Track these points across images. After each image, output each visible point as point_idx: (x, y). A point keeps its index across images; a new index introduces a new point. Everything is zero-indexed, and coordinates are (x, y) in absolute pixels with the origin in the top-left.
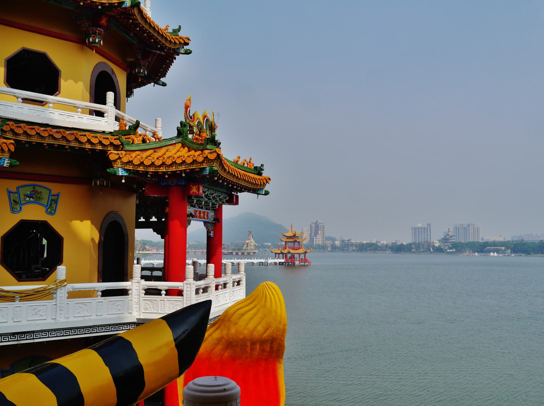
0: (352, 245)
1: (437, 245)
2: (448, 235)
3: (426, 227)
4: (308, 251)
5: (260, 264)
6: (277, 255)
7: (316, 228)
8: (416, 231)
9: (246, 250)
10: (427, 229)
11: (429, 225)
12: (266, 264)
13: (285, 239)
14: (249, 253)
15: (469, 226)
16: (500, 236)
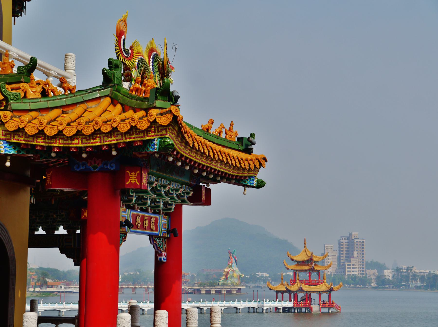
0: (415, 277)
4: (335, 287)
5: (250, 310)
6: (280, 295)
9: (224, 285)
13: (293, 266)
14: (229, 292)
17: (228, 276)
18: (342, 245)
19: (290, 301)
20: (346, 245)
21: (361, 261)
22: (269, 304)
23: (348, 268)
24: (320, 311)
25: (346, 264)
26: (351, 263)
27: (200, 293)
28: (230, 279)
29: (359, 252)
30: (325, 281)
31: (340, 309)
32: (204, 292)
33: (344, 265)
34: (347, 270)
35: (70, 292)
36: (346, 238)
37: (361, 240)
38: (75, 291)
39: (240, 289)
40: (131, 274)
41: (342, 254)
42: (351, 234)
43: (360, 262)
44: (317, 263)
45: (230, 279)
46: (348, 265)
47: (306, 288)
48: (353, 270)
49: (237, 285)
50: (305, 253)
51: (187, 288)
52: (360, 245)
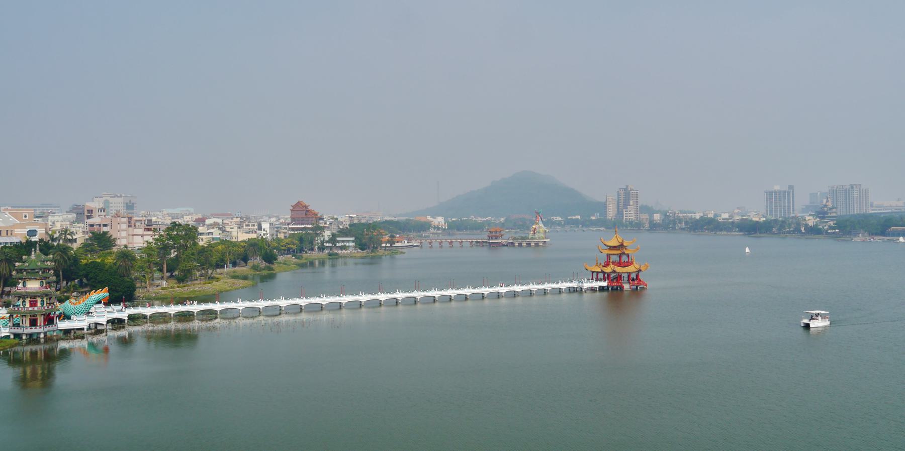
0: (680, 221)
1: (811, 224)
2: (826, 206)
3: (786, 189)
6: (595, 275)
7: (626, 197)
8: (771, 196)
9: (532, 238)
10: (788, 194)
11: (791, 187)
14: (537, 244)
15: (852, 187)
16: (899, 200)
47: (619, 269)
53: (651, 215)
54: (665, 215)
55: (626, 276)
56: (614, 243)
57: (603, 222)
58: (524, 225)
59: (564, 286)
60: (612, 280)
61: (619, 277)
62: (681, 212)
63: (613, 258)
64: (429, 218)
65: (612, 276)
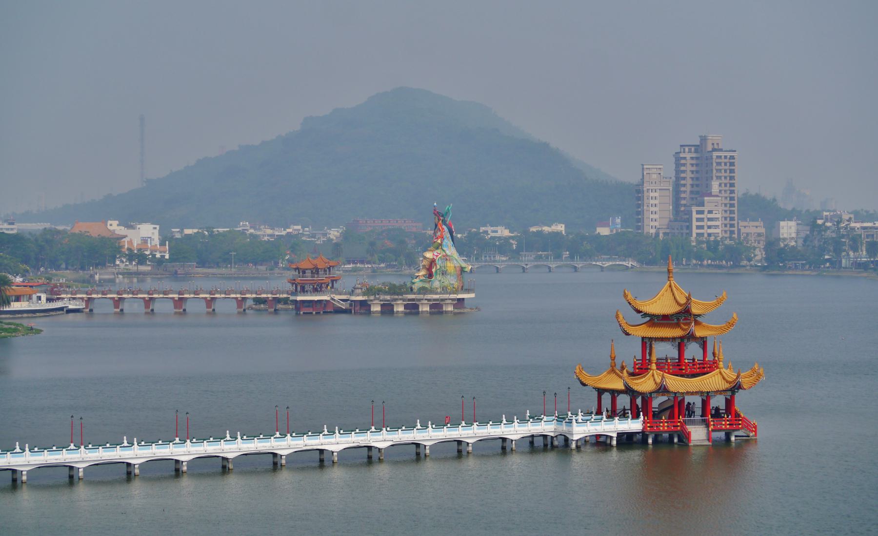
4: (745, 381)
5: (537, 446)
7: (700, 168)
9: (423, 290)
12: (560, 446)
14: (437, 307)
17: (434, 270)
18: (684, 165)
19: (636, 416)
20: (692, 165)
21: (727, 201)
22: (585, 428)
23: (698, 220)
24: (709, 439)
25: (694, 209)
26: (706, 209)
27: (369, 312)
28: (439, 278)
29: (724, 181)
30: (721, 364)
31: (755, 432)
32: (378, 309)
33: (690, 213)
34: (695, 223)
35: (61, 309)
36: (693, 149)
37: (729, 154)
38: (71, 307)
39: (463, 299)
40: (188, 236)
41: (684, 185)
42: (704, 139)
43: (726, 205)
44: (698, 319)
45: (439, 278)
46: (698, 212)
48: (710, 223)
49: (456, 292)
50: (669, 290)
51: (337, 297)
52: (725, 164)
53: (772, 225)
54: (812, 223)
55: (697, 401)
56: (662, 304)
57: (631, 245)
58: (402, 252)
59: (515, 431)
60: (657, 415)
61: (678, 407)
62: (858, 216)
63: (664, 351)
64: (114, 226)
65: (656, 403)
